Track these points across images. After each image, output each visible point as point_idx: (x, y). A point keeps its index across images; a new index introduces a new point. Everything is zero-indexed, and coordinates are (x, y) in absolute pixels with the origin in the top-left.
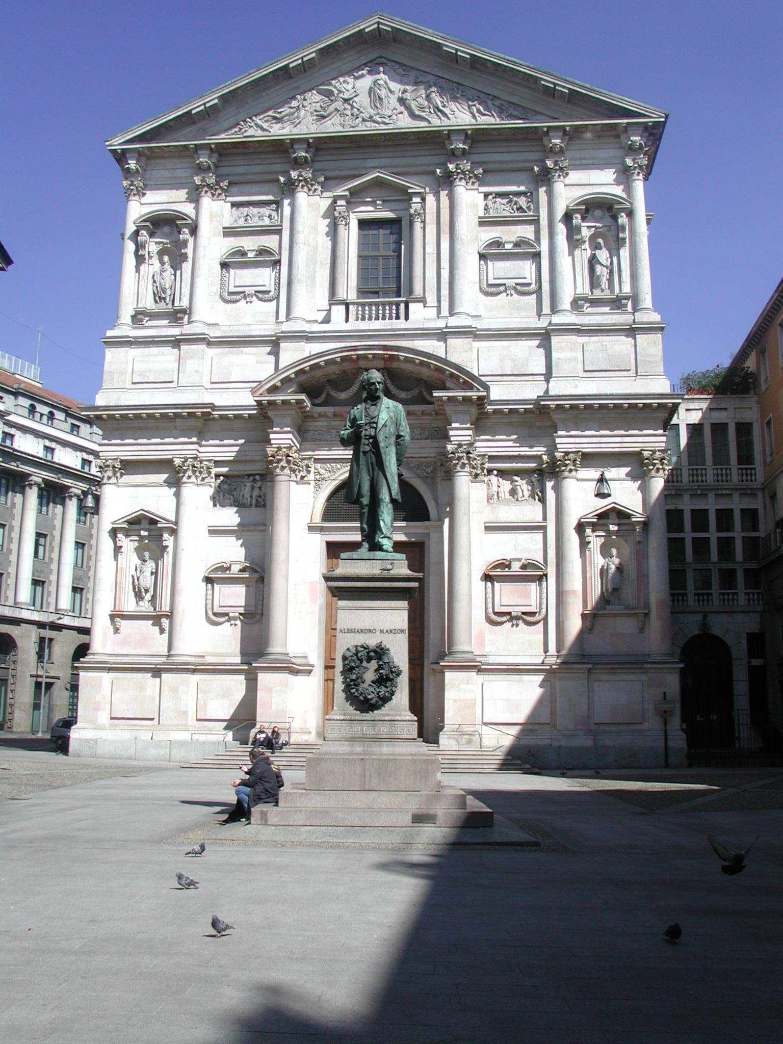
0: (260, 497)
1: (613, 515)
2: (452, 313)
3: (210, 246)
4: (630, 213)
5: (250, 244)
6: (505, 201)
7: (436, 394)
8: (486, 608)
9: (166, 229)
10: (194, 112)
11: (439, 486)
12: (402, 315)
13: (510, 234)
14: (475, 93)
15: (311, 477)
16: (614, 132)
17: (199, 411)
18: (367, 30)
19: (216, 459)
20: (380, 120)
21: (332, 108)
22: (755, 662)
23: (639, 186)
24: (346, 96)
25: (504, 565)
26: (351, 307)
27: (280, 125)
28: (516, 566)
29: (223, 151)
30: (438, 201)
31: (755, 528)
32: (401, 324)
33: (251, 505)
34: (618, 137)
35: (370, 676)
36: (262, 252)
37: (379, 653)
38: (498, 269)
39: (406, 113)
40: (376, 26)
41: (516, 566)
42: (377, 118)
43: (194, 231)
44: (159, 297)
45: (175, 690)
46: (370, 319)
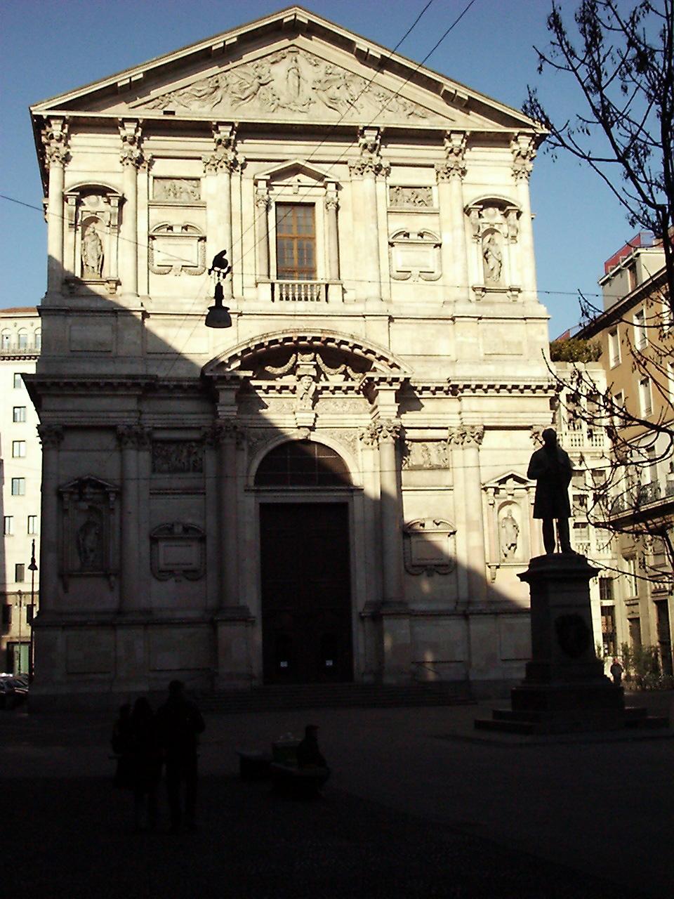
0: (195, 461)
3: (140, 218)
4: (519, 214)
5: (177, 218)
6: (407, 192)
9: (93, 198)
10: (119, 85)
11: (359, 453)
12: (323, 297)
13: (414, 224)
14: (382, 90)
15: (245, 445)
16: (502, 140)
17: (143, 382)
18: (285, 21)
19: (155, 426)
20: (294, 108)
21: (247, 93)
24: (261, 81)
26: (277, 287)
27: (198, 103)
29: (150, 128)
33: (188, 470)
34: (508, 142)
36: (186, 228)
38: (402, 257)
39: (319, 102)
40: (293, 17)
42: (292, 106)
43: (122, 201)
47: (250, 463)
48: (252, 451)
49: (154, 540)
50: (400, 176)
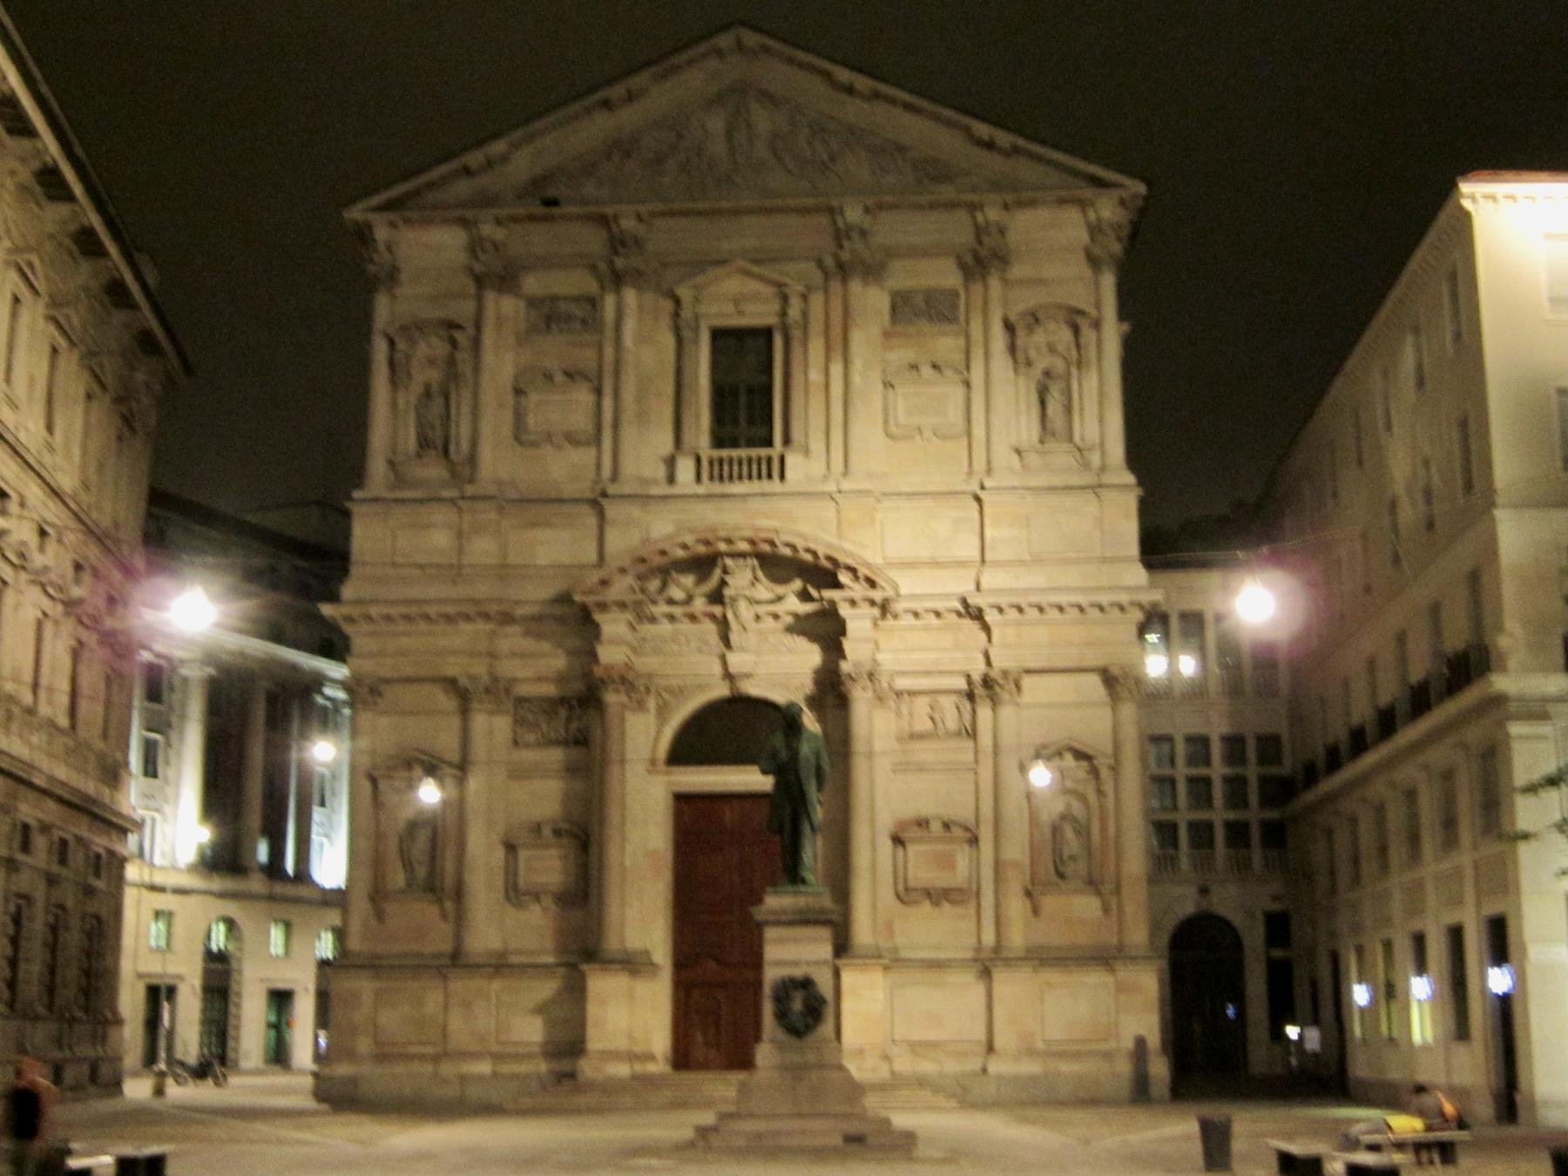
1: (1069, 757)
2: (846, 472)
3: (500, 363)
7: (829, 594)
8: (896, 884)
15: (652, 703)
22: (1278, 953)
23: (1108, 281)
25: (923, 823)
28: (936, 827)
30: (827, 302)
31: (1277, 759)
32: (775, 486)
35: (797, 1005)
37: (806, 984)
41: (936, 827)
44: (424, 443)
45: (467, 1005)
46: (731, 477)
47: (659, 733)
48: (663, 712)
49: (511, 848)
50: (904, 276)
